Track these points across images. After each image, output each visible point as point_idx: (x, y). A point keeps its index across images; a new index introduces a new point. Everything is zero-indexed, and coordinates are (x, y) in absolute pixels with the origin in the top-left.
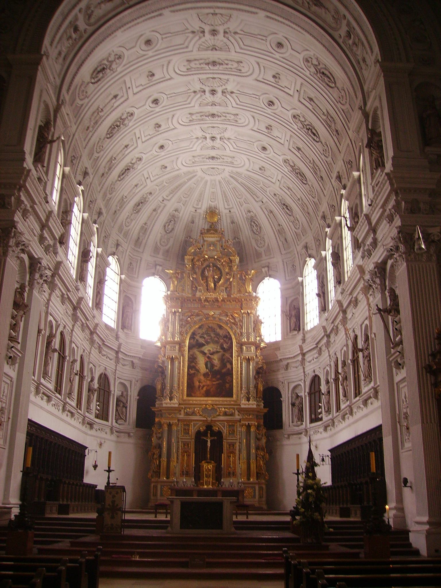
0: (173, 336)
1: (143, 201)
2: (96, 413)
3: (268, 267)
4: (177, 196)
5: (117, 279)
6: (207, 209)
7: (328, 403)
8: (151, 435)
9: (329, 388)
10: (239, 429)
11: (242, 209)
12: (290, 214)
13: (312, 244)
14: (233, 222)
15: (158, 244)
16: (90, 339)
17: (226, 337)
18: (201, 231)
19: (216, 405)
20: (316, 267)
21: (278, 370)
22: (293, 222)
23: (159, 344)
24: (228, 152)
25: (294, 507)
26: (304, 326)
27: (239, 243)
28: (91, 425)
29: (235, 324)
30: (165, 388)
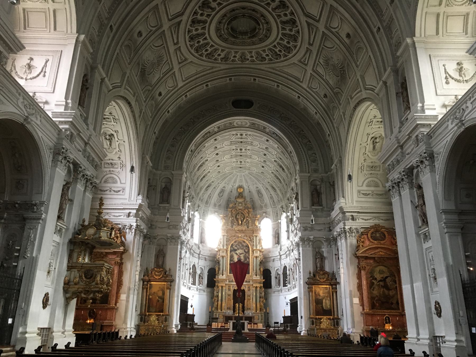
0: (223, 247)
3: (266, 213)
4: (224, 182)
13: (284, 206)
14: (250, 192)
17: (246, 246)
21: (270, 261)
22: (277, 195)
23: (217, 250)
24: (247, 166)
27: (253, 201)
28: (190, 288)
29: (251, 241)
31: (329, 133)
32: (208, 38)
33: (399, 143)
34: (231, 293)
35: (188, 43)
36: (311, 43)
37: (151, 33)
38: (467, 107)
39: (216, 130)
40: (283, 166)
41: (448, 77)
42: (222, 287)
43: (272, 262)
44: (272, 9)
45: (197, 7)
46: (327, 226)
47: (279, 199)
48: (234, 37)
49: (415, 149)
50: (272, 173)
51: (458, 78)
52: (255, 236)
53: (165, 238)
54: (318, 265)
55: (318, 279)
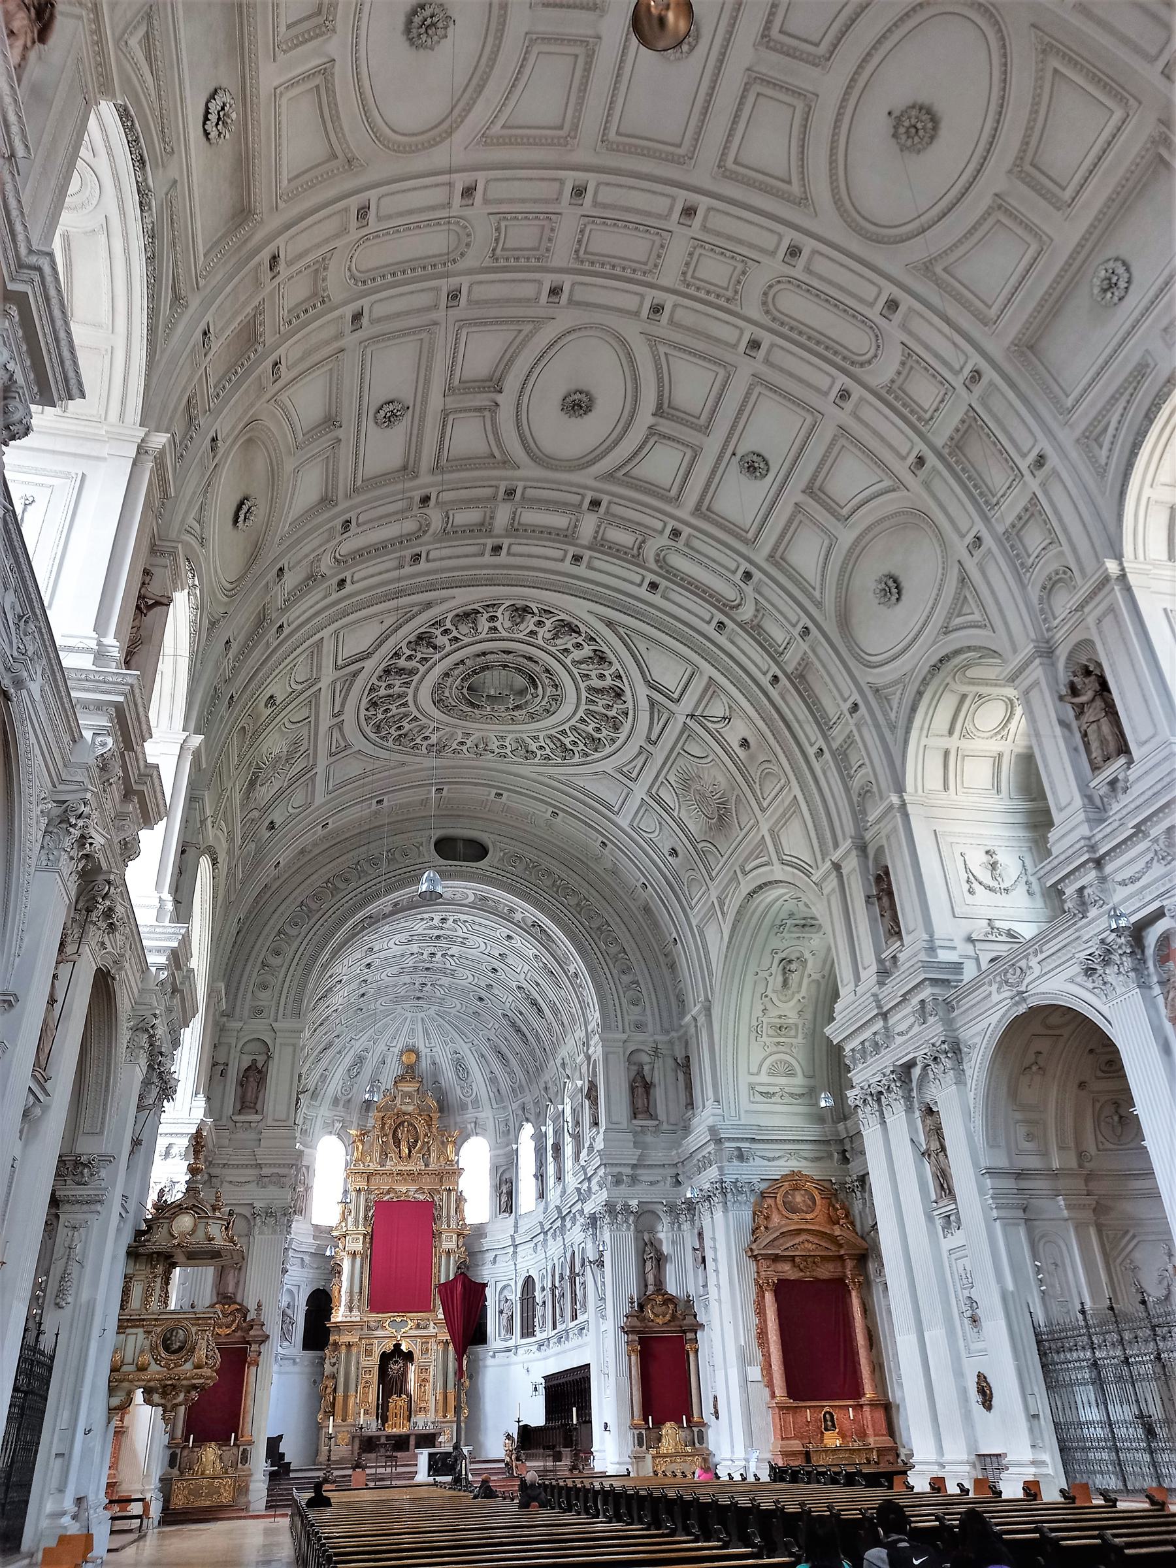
0: (356, 1222)
14: (434, 1064)
31: (675, 935)
32: (411, 703)
33: (879, 1007)
34: (374, 1362)
35: (363, 712)
36: (653, 737)
37: (293, 695)
38: (1031, 968)
39: (387, 910)
40: (540, 1001)
41: (971, 879)
42: (349, 1345)
43: (488, 1266)
44: (573, 661)
45: (404, 645)
46: (673, 1171)
47: (516, 1086)
48: (472, 705)
49: (916, 1029)
50: (504, 1015)
51: (992, 883)
52: (445, 1190)
53: (249, 1215)
54: (651, 1278)
55: (651, 1316)
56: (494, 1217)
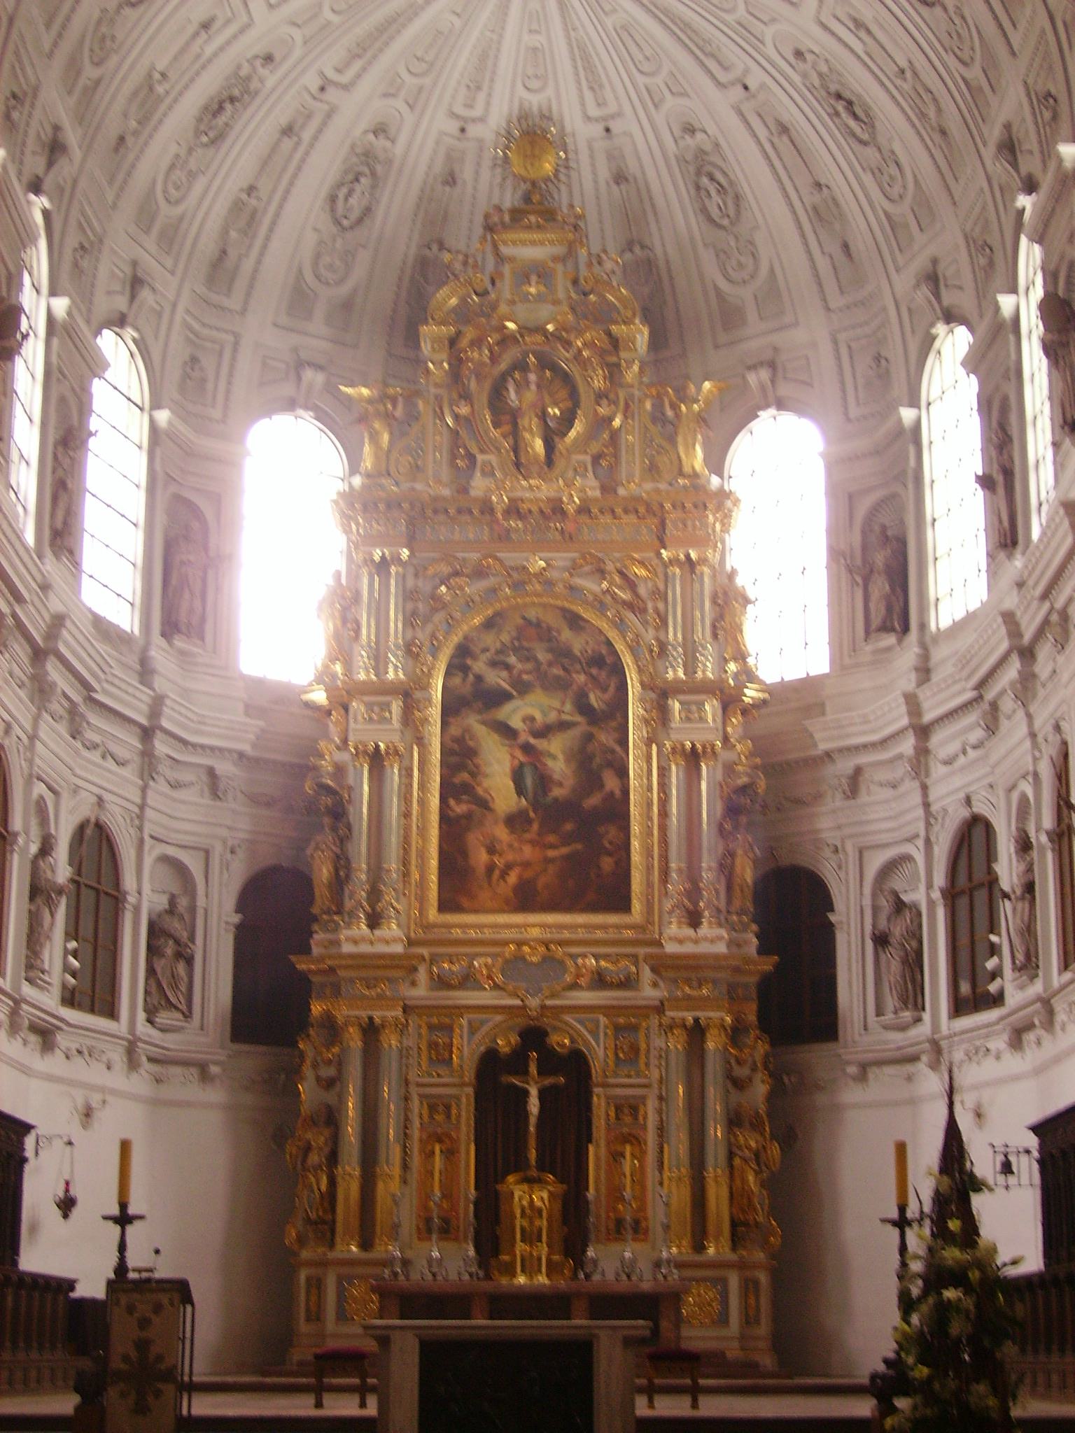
1: (236, 92)
2: (64, 986)
3: (772, 365)
5: (138, 428)
6: (509, 122)
7: (1029, 931)
8: (294, 1073)
9: (1030, 869)
10: (658, 1042)
11: (659, 119)
12: (865, 137)
13: (959, 266)
14: (620, 178)
15: (309, 276)
16: (33, 678)
17: (597, 661)
18: (487, 216)
19: (561, 943)
20: (975, 362)
22: (877, 172)
23: (319, 696)
25: (886, 1361)
26: (923, 609)
28: (45, 1035)
29: (636, 607)
30: (348, 876)
43: (834, 801)
47: (901, 210)
52: (674, 561)
56: (843, 650)
